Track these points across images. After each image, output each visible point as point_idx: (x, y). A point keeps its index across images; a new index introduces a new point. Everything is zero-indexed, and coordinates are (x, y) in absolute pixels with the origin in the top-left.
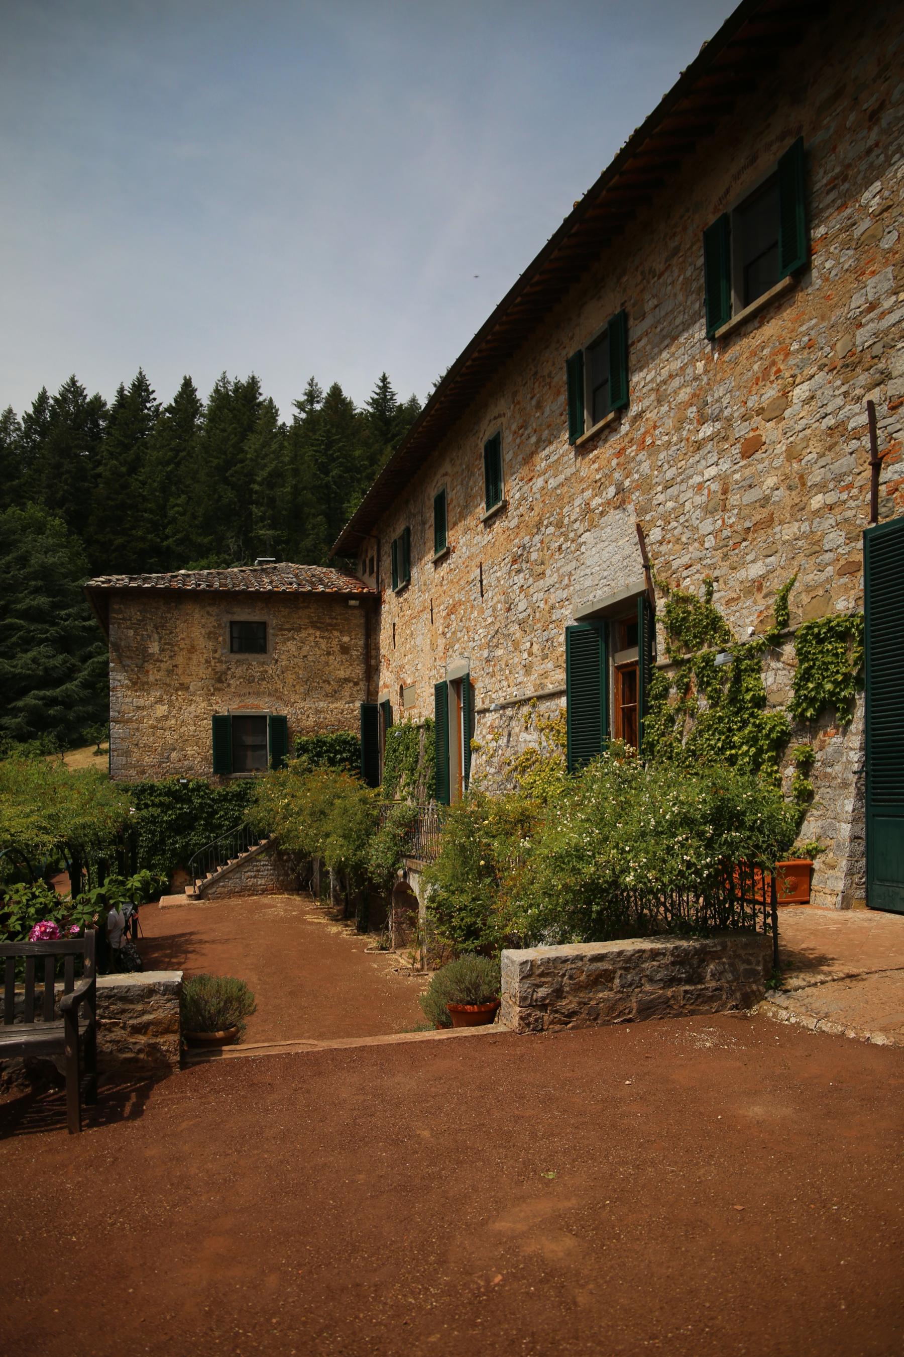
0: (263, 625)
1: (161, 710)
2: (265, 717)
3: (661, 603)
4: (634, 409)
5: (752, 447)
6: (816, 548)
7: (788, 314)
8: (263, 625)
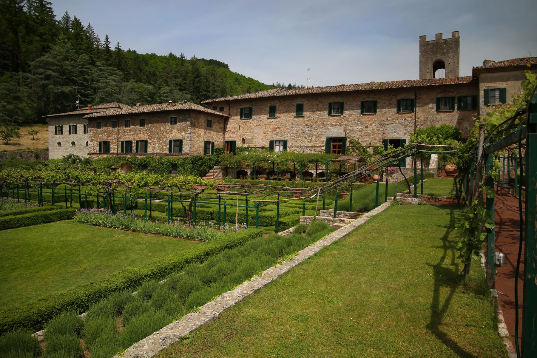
0: (211, 121)
1: (197, 139)
2: (210, 142)
3: (348, 139)
4: (344, 115)
5: (367, 127)
6: (375, 139)
7: (373, 116)
8: (211, 121)
